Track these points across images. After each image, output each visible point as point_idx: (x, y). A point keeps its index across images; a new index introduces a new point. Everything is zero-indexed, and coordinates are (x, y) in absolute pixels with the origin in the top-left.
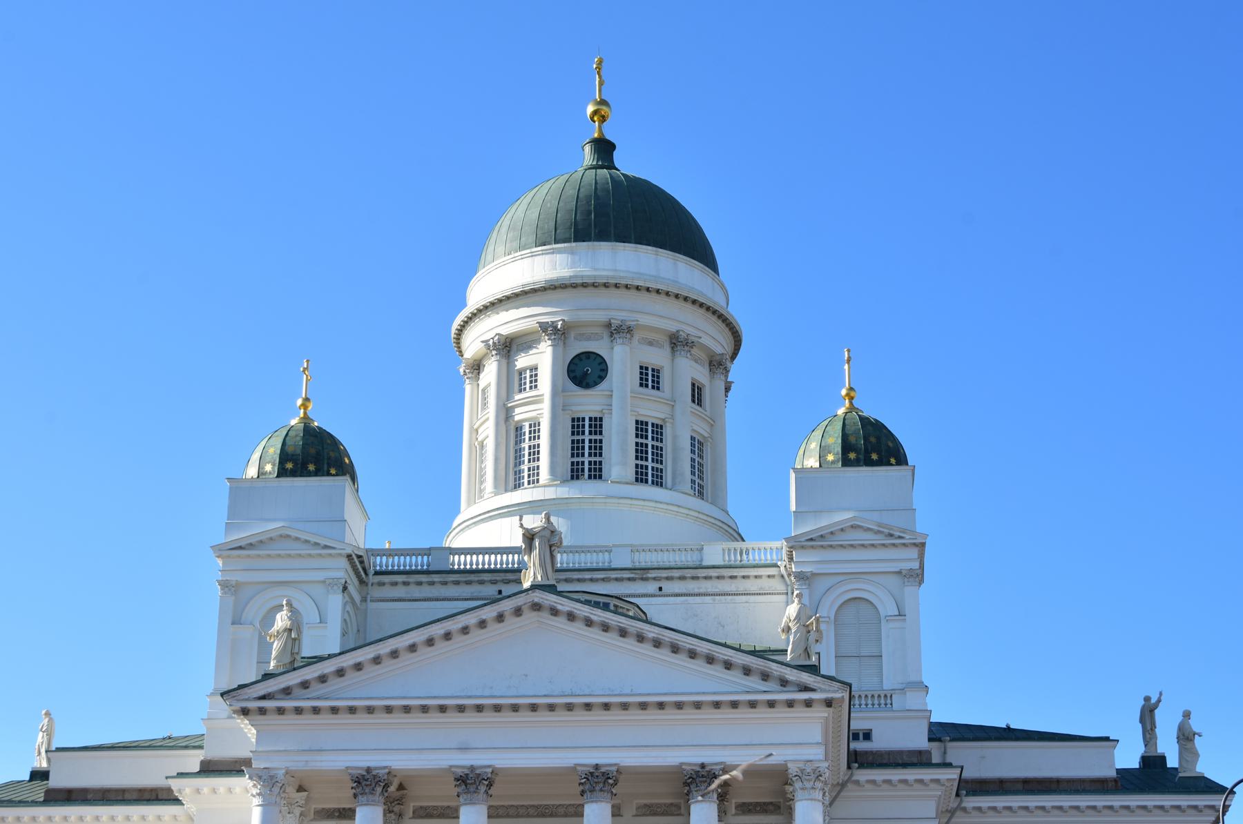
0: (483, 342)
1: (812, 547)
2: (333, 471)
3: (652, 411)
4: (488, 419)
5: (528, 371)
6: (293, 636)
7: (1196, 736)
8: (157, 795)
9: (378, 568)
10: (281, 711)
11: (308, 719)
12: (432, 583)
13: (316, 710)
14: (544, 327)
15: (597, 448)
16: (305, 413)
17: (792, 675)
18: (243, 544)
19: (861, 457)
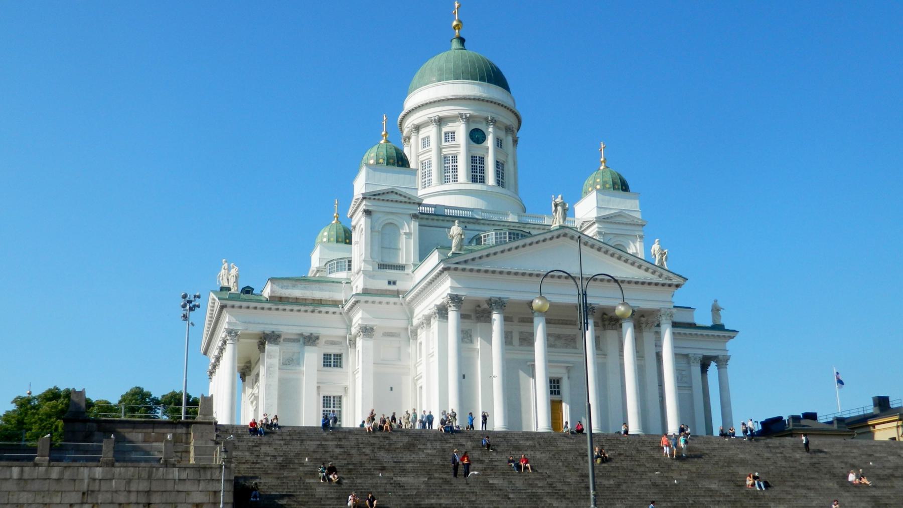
0: (428, 118)
1: (604, 222)
2: (407, 166)
3: (502, 159)
4: (431, 151)
5: (450, 135)
6: (463, 237)
7: (722, 310)
8: (321, 303)
9: (421, 212)
10: (464, 270)
11: (474, 274)
12: (437, 220)
13: (479, 271)
14: (461, 115)
15: (482, 170)
16: (386, 138)
17: (665, 274)
18: (375, 193)
19: (620, 187)
